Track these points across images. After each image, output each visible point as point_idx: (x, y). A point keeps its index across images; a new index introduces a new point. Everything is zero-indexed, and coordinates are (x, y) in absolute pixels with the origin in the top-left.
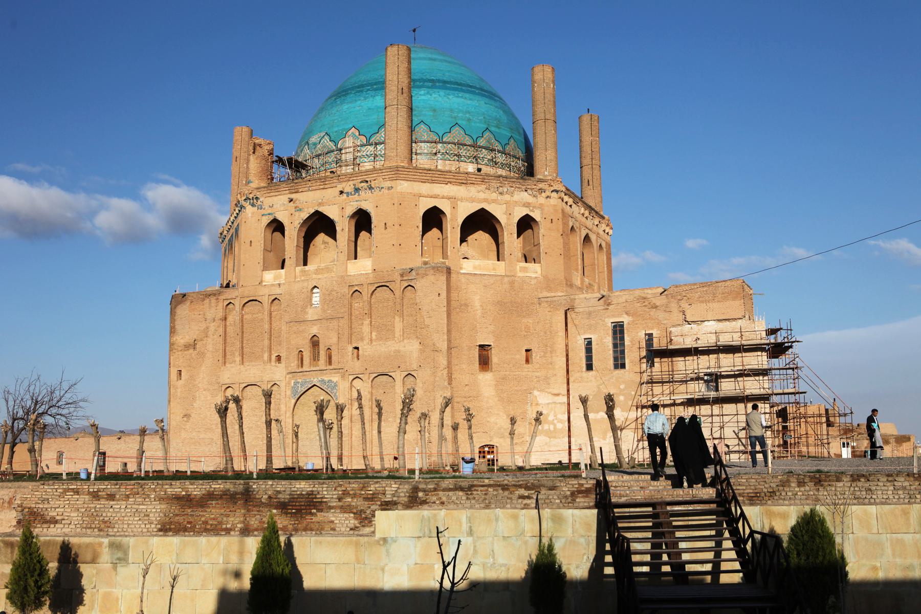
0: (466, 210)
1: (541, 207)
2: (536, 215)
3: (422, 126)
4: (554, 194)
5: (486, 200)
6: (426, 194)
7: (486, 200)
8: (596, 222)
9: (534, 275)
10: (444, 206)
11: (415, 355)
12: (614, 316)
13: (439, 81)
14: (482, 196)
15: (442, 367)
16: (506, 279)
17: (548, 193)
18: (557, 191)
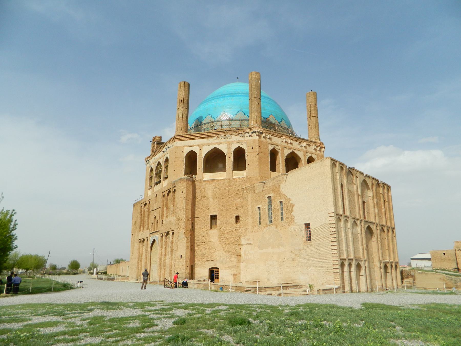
0: (206, 150)
1: (246, 142)
2: (244, 146)
3: (209, 116)
4: (254, 134)
5: (216, 143)
6: (187, 145)
7: (216, 143)
8: (304, 144)
9: (241, 177)
10: (196, 150)
11: (174, 222)
12: (269, 193)
13: (223, 95)
14: (215, 141)
15: (182, 227)
16: (226, 181)
17: (251, 134)
18: (255, 132)
